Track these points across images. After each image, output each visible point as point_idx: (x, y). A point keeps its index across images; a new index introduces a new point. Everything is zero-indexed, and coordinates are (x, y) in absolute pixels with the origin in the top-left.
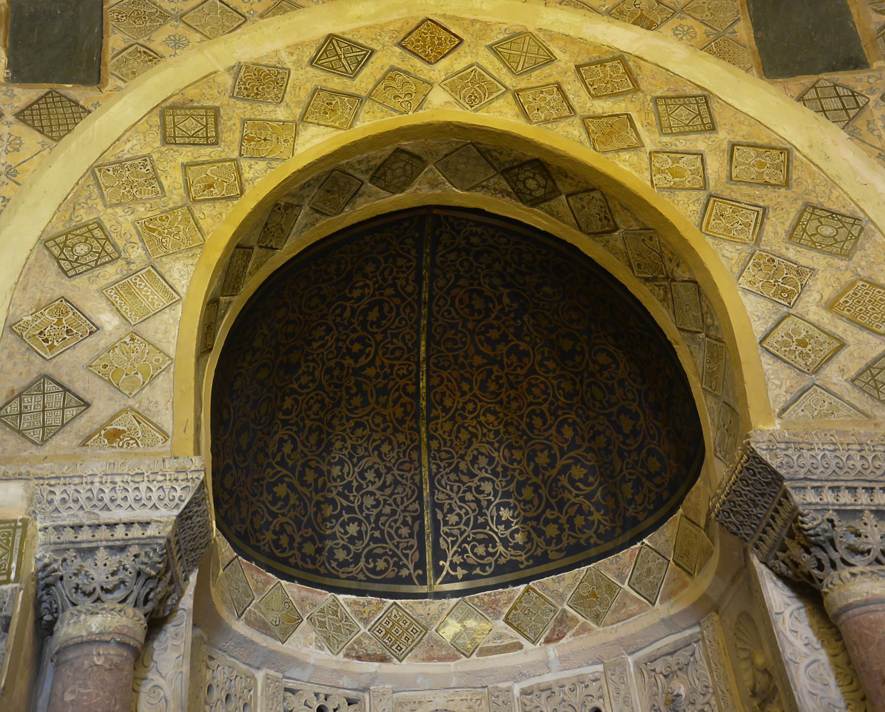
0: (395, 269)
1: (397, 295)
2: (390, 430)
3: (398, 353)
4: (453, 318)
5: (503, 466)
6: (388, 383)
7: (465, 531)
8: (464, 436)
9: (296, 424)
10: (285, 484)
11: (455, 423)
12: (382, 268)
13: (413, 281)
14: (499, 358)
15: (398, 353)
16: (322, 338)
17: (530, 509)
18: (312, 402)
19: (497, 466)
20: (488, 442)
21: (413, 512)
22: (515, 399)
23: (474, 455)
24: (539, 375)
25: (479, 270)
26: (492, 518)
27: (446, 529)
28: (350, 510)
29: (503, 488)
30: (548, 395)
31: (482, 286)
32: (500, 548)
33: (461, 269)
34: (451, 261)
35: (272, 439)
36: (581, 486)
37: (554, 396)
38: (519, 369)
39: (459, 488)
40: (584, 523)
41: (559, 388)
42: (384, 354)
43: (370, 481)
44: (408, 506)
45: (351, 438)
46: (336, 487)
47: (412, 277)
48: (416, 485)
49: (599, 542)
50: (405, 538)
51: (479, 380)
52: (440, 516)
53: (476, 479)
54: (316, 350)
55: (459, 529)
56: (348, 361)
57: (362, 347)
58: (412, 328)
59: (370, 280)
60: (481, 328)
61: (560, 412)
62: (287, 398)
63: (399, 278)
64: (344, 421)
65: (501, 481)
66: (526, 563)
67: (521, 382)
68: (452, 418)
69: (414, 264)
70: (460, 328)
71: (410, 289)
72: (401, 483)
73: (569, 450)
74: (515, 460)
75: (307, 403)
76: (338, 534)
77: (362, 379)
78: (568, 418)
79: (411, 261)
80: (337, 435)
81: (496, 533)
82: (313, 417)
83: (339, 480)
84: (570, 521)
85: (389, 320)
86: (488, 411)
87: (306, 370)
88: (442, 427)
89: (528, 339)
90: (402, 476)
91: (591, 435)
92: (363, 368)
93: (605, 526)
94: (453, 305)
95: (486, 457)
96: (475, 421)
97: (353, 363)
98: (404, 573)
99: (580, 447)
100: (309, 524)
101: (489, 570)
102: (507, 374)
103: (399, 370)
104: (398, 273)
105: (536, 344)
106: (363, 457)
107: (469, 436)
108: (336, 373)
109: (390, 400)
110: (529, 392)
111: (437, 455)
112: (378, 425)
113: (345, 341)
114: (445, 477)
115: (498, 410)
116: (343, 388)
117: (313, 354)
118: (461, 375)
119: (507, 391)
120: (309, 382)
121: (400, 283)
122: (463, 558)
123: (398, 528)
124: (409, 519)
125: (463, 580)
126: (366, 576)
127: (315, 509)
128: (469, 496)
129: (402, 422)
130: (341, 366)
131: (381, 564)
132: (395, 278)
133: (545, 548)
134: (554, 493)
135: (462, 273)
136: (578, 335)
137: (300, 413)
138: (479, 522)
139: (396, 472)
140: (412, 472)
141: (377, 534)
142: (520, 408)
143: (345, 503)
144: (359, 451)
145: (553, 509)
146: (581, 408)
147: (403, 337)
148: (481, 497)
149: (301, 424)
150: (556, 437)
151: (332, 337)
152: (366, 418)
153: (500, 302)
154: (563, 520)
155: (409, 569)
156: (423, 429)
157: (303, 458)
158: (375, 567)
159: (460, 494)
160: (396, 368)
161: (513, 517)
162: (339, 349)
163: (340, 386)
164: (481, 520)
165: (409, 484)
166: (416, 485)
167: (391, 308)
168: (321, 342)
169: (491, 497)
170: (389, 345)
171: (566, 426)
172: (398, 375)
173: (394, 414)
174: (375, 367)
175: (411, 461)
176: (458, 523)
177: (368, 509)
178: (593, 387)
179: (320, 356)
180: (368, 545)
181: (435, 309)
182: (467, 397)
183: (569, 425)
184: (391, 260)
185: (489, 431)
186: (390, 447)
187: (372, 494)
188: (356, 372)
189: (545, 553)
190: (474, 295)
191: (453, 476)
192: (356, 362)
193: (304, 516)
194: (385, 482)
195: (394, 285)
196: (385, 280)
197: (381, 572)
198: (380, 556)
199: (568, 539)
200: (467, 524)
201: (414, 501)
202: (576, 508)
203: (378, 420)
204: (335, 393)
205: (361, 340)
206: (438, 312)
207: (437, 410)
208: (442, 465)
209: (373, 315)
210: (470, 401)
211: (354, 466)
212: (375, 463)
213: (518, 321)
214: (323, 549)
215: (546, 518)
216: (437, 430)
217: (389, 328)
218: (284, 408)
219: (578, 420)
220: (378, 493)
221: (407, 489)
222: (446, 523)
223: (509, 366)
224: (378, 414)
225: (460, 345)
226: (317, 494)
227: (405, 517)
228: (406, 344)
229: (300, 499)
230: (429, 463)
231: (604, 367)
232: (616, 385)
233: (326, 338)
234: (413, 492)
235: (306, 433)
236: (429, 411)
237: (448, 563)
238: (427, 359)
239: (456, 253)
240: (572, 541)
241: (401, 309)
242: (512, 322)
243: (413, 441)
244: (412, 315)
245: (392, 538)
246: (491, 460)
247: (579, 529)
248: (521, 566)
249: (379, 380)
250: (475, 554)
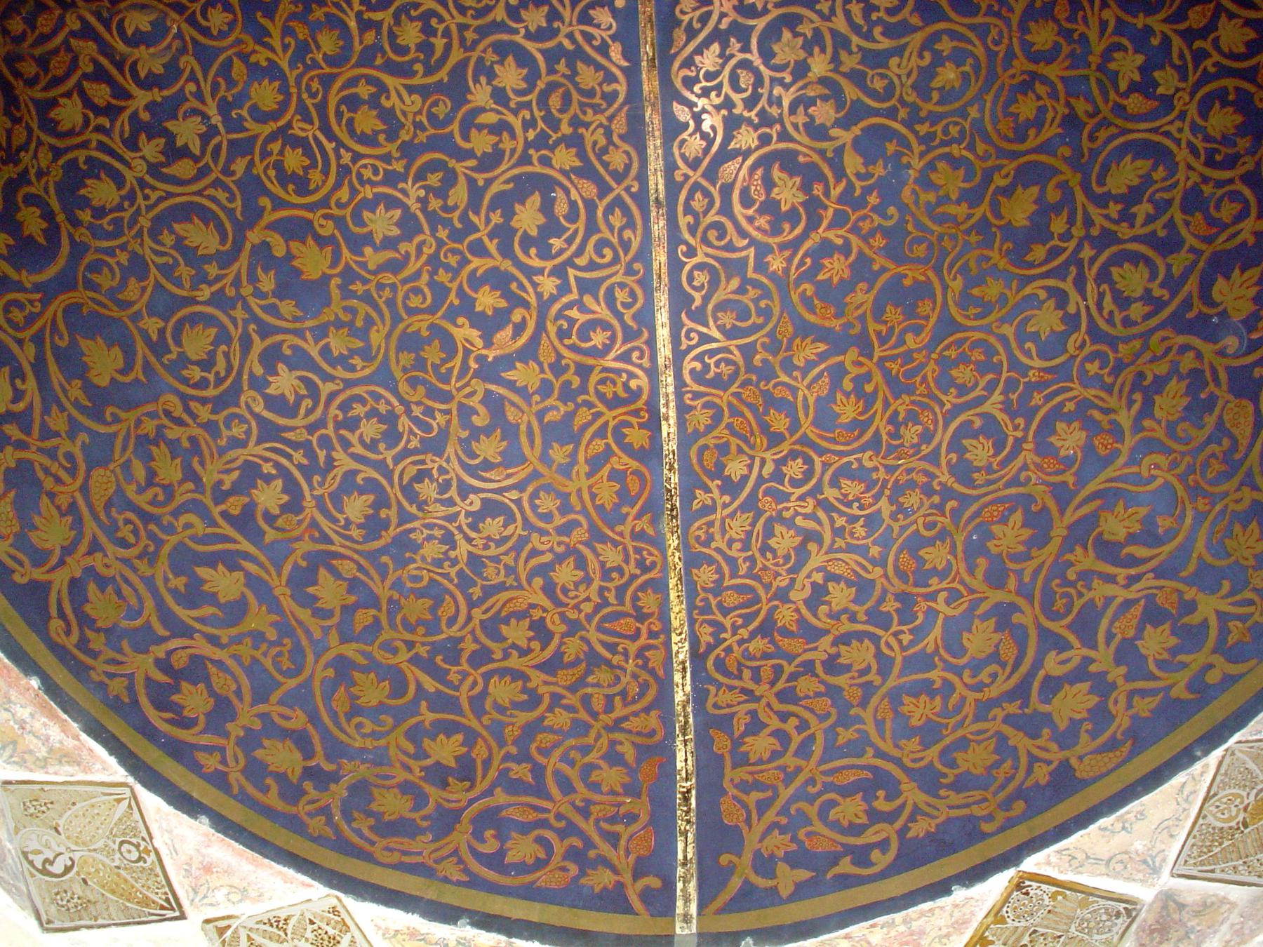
0: (575, 96)
1: (586, 171)
2: (580, 535)
3: (598, 338)
4: (730, 247)
5: (900, 597)
6: (571, 415)
7: (799, 770)
8: (784, 541)
9: (306, 446)
11: (759, 514)
12: (541, 85)
13: (621, 137)
14: (856, 330)
15: (598, 338)
16: (390, 243)
17: (994, 676)
18: (359, 410)
19: (881, 600)
20: (850, 549)
22: (912, 417)
23: (814, 584)
24: (966, 329)
25: (777, 91)
26: (879, 724)
27: (742, 774)
28: (443, 703)
29: (903, 649)
30: (998, 370)
31: (791, 139)
32: (912, 794)
33: (737, 98)
34: (710, 76)
35: (222, 452)
36: (1141, 552)
37: (1014, 364)
38: (909, 338)
39: (778, 670)
40: (1173, 641)
41: (1021, 337)
42: (562, 334)
43: (514, 646)
44: (626, 718)
45: (469, 540)
46: (410, 645)
47: (620, 126)
49: (1234, 669)
50: (612, 792)
51: (811, 401)
52: (722, 743)
53: (825, 643)
54: (374, 273)
55: (782, 768)
56: (464, 332)
57: (503, 304)
58: (629, 272)
59: (515, 113)
60: (802, 263)
61: (1037, 399)
62: (281, 367)
63: (587, 125)
64: (453, 493)
65: (895, 634)
66: (1001, 816)
67: (923, 366)
68: (751, 505)
69: (622, 88)
70: (750, 274)
71: (617, 159)
72: (608, 663)
73: (1081, 482)
74: (934, 571)
75: (345, 407)
76: (393, 751)
77: (501, 391)
78: (1062, 404)
79: (616, 81)
80: (430, 526)
81: (898, 762)
82: (358, 449)
84: (1127, 653)
85: (569, 242)
86: (845, 472)
87: (345, 317)
88: (724, 531)
89: (920, 251)
90: (612, 648)
91: (1136, 407)
92: (507, 361)
93: (1242, 618)
94: (726, 210)
95: (849, 584)
96: (811, 501)
97: (479, 343)
98: (601, 879)
99: (1108, 461)
100: (301, 697)
101: (880, 860)
102: (882, 359)
103: (602, 382)
104: (581, 105)
105: (944, 253)
106: (502, 587)
107: (798, 540)
108: (433, 354)
109: (581, 457)
110: (945, 382)
111: (714, 603)
112: (547, 517)
113: (456, 272)
114: (737, 652)
115: (869, 464)
116: (453, 406)
117: (366, 282)
118: (765, 394)
119: (886, 404)
120: (353, 352)
121: (595, 137)
122: (794, 839)
123: (589, 769)
124: (628, 751)
125: (793, 898)
126: (466, 871)
127: (330, 672)
128: (806, 685)
129: (613, 518)
130: (449, 346)
131: (522, 849)
132: (576, 123)
133: (1056, 755)
134: (1060, 604)
135: (736, 111)
136: (1043, 158)
137: (321, 424)
138: (841, 740)
139: (593, 635)
140: (643, 640)
141: (521, 771)
142: (926, 437)
143: (430, 684)
144: (490, 570)
145: (1063, 646)
146: (1090, 358)
147: (610, 293)
148: (841, 680)
149: (322, 455)
150: (1039, 467)
151: (419, 252)
152: (514, 495)
153: (840, 173)
154: (1103, 659)
155: (615, 871)
156: (673, 541)
157: (312, 538)
158: (501, 853)
159: (780, 685)
160: (594, 378)
161: (945, 713)
162: (440, 292)
163: (446, 397)
164: (845, 735)
165: (630, 667)
166: (652, 672)
167: (573, 204)
168: (390, 254)
169: (873, 677)
170: (574, 313)
171: (1060, 426)
172: (601, 396)
173: (593, 496)
174: (540, 365)
175: (641, 617)
176: (775, 755)
177: (500, 709)
178: (1115, 271)
179: (387, 293)
180: (489, 792)
181: (684, 221)
182: (785, 448)
183: (1069, 418)
184: (562, 67)
185: (853, 519)
187: (517, 675)
188: (489, 372)
189: (1065, 766)
190: (777, 174)
191: (757, 645)
192: (488, 344)
193: (289, 674)
194: (559, 654)
195: (575, 142)
196: (554, 124)
197: (523, 868)
198: (525, 829)
199: (1129, 705)
200: (804, 750)
201: (647, 710)
202: (1137, 610)
203: (548, 503)
204: (429, 412)
205: (499, 280)
206: (692, 229)
207: (708, 490)
208: (728, 622)
209: (528, 218)
210: (793, 455)
211: (471, 605)
212: (532, 606)
213: (892, 210)
215: (1048, 678)
216: (710, 538)
217: (570, 262)
218: (270, 391)
219: (1090, 393)
220: (537, 678)
222: (741, 760)
223: (883, 340)
224: (548, 488)
225: (754, 319)
226: (344, 640)
227: (613, 743)
228: (619, 316)
229: (285, 629)
230: (692, 622)
231: (1132, 196)
232: (1179, 218)
233: (403, 247)
234: (644, 687)
235: (333, 481)
236: (688, 497)
237: (747, 856)
238: (679, 356)
239: (716, 47)
240: (1144, 706)
241: (600, 213)
242: (877, 220)
243: (641, 564)
244: (628, 234)
245: (566, 787)
246: (862, 587)
247: (1161, 664)
248: (987, 827)
249: (550, 402)
250: (835, 825)
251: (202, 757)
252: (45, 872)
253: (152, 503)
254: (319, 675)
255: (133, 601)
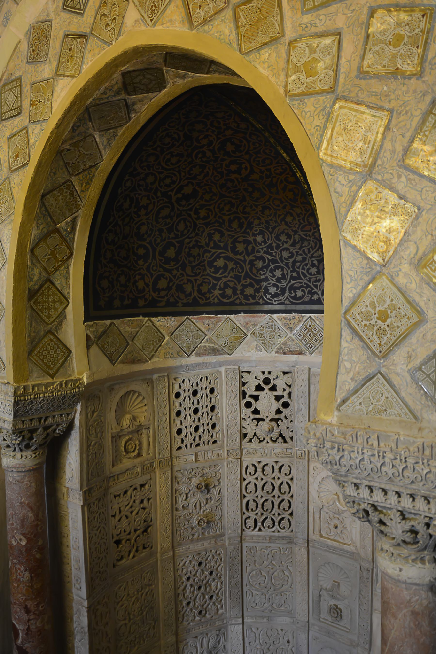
10: (222, 259)
21: (317, 257)
48: (317, 239)
72: (306, 239)
83: (263, 244)
90: (306, 235)
103: (275, 170)
123: (309, 269)
160: (272, 170)
166: (317, 239)
173: (287, 197)
175: (310, 224)
186: (292, 218)
214: (261, 288)
221: (311, 243)
251: (236, 302)
252: (225, 346)
253: (198, 260)
254: (248, 268)
255: (208, 281)
